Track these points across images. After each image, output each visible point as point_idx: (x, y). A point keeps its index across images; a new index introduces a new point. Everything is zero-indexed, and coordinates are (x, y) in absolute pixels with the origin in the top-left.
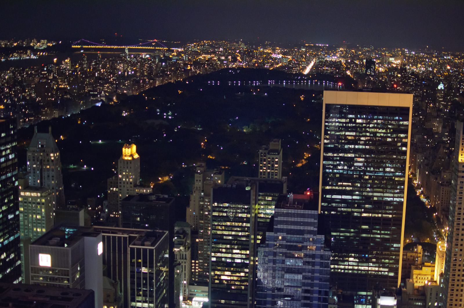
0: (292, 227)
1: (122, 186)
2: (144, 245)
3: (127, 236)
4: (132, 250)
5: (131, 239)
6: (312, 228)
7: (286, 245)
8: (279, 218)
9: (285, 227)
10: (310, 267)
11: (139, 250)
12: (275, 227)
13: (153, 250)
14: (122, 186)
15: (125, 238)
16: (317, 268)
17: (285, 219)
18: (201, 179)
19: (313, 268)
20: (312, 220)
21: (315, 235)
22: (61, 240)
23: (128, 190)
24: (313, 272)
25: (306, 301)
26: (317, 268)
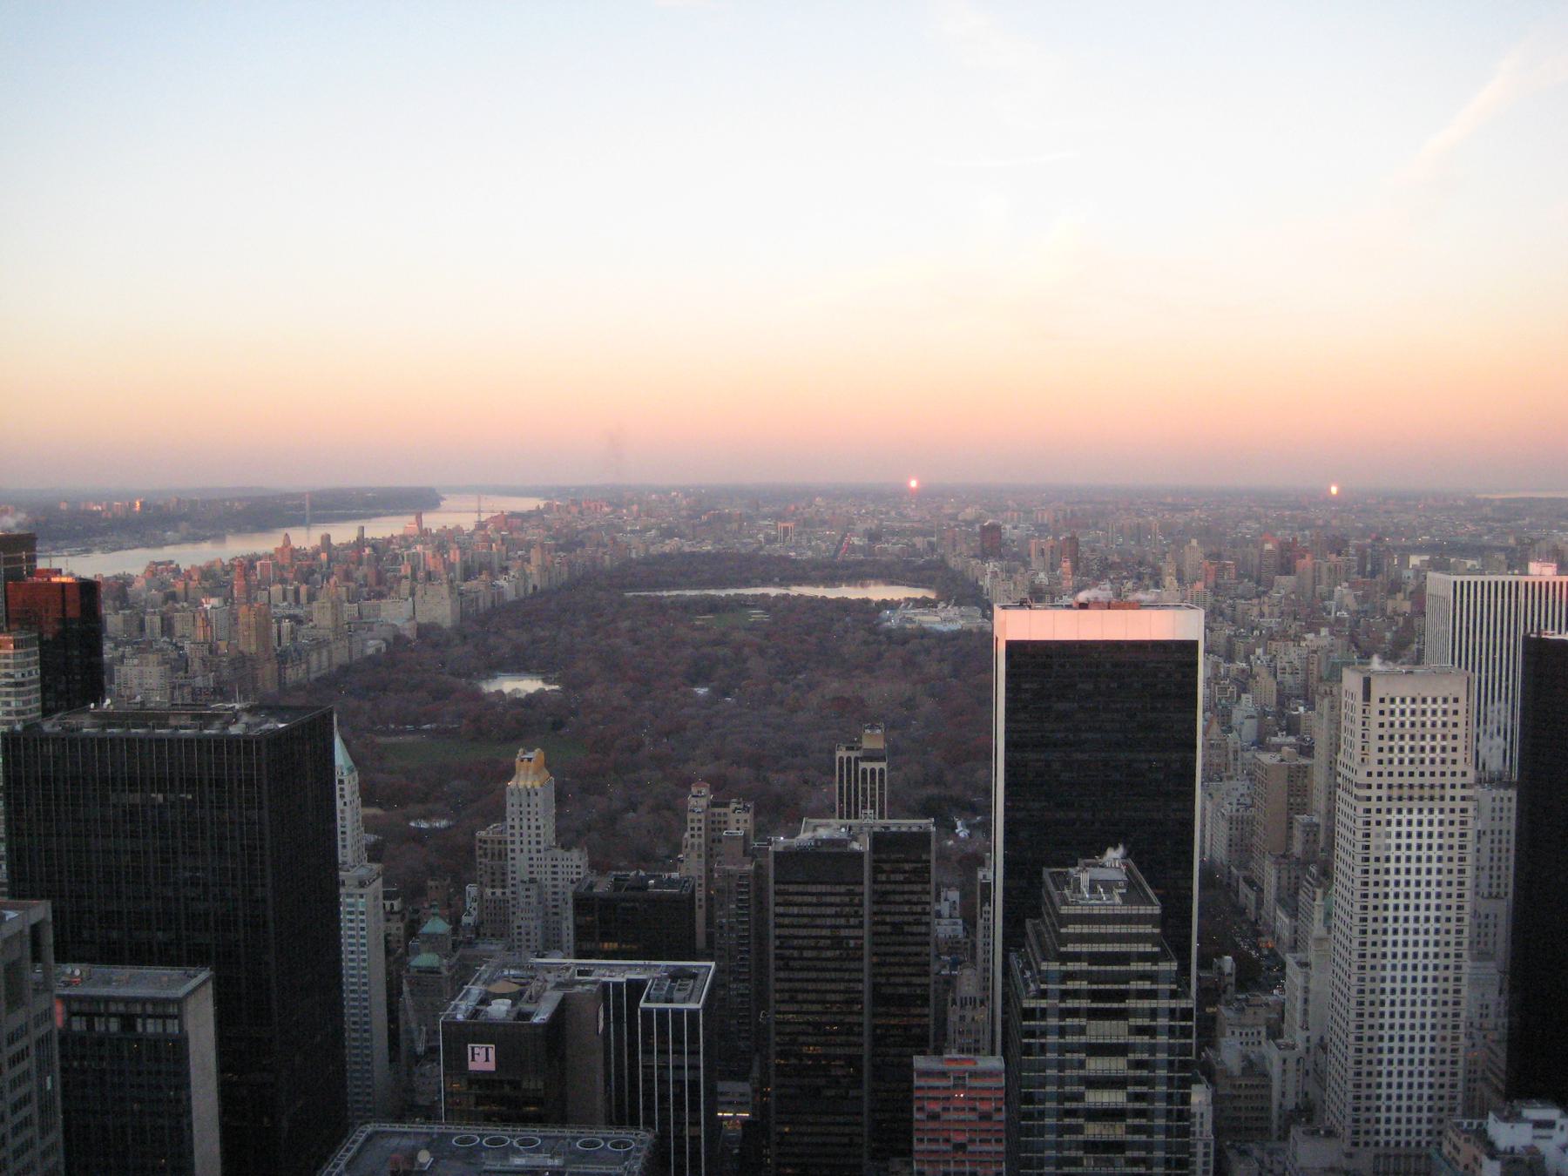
0: (1103, 948)
1: (518, 851)
2: (671, 1001)
3: (620, 978)
4: (647, 1013)
5: (636, 987)
6: (1148, 948)
7: (1089, 990)
8: (1072, 929)
9: (1085, 948)
10: (1146, 1039)
11: (662, 1013)
12: (1063, 949)
13: (698, 1010)
14: (518, 851)
15: (617, 985)
16: (1162, 1039)
17: (1086, 929)
18: (702, 825)
19: (1153, 1041)
20: (1148, 929)
21: (1155, 963)
22: (513, 1005)
23: (531, 859)
24: (1152, 1049)
25: (1137, 1121)
26: (1162, 1039)
